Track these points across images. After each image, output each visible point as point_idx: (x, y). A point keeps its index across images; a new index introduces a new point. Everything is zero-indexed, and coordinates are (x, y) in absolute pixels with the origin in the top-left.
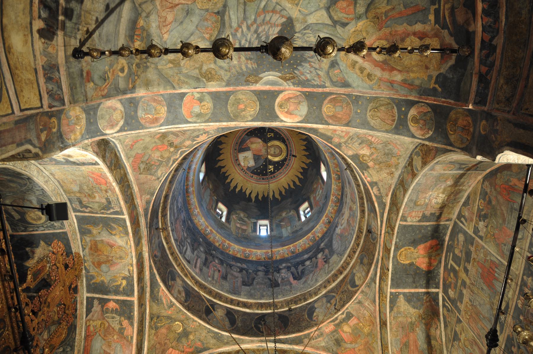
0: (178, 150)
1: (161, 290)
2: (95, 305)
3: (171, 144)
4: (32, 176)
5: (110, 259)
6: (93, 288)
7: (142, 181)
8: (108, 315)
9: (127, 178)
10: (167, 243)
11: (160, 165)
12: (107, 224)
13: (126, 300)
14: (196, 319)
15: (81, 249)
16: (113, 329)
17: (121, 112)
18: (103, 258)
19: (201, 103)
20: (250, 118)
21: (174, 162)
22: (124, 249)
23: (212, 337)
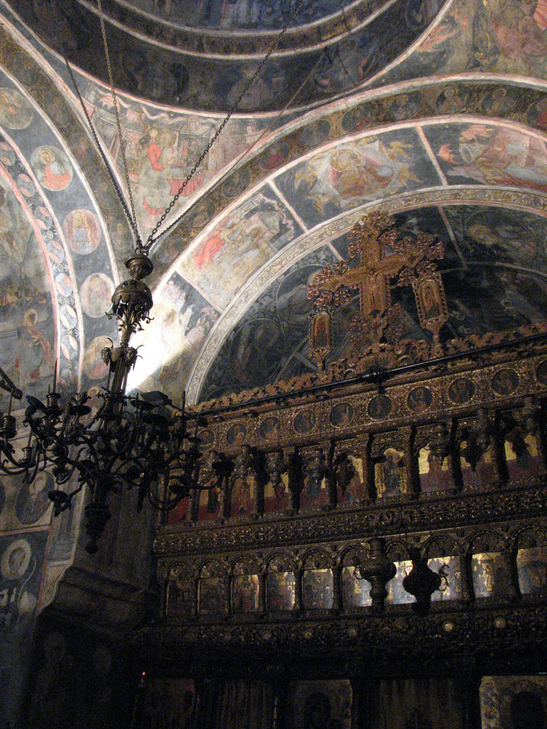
0: (152, 122)
1: (421, 50)
2: (458, 174)
3: (144, 142)
5: (363, 169)
7: (221, 156)
8: (464, 158)
9: (216, 190)
10: (371, 12)
11: (188, 138)
13: (427, 136)
16: (485, 151)
19: (45, 165)
20: (16, 93)
21: (176, 115)
22: (335, 158)
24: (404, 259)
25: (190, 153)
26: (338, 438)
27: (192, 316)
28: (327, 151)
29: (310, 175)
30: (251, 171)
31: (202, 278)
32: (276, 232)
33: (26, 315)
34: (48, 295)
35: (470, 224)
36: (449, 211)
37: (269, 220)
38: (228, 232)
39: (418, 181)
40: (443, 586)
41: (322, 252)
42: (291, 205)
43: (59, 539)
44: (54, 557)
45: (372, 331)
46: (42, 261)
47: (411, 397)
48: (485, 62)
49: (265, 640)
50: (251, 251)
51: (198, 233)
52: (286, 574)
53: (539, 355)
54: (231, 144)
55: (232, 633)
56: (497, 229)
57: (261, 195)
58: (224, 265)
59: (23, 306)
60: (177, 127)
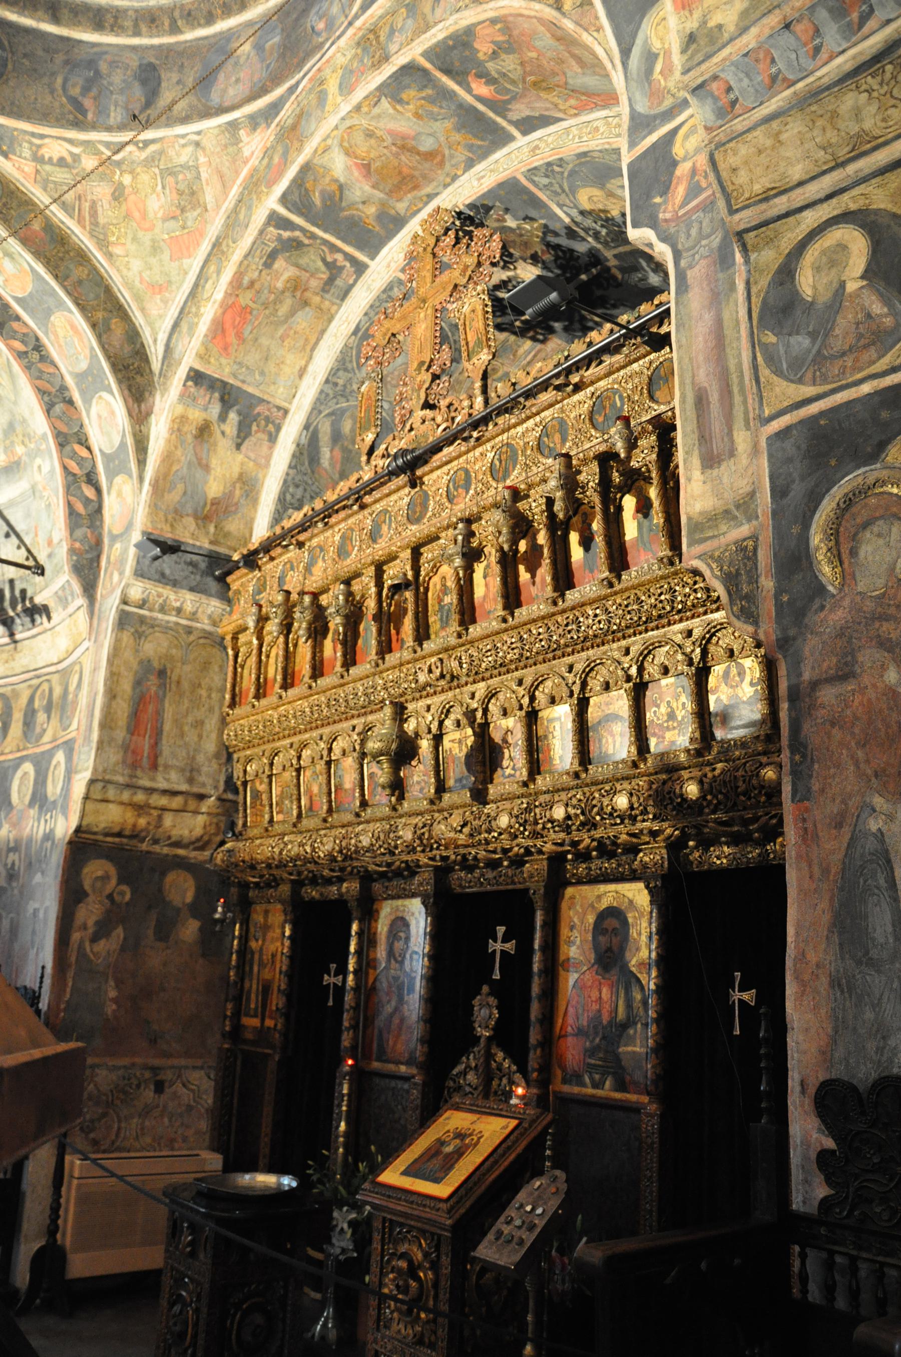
3: (118, 194)
5: (394, 148)
7: (219, 186)
11: (170, 172)
24: (457, 273)
25: (180, 193)
27: (240, 423)
28: (328, 136)
29: (327, 180)
31: (236, 367)
32: (325, 277)
35: (573, 191)
37: (303, 261)
38: (249, 294)
40: (505, 763)
41: (396, 289)
42: (325, 231)
47: (451, 485)
50: (300, 313)
52: (350, 759)
53: (592, 383)
54: (227, 164)
56: (608, 186)
57: (271, 229)
58: (264, 341)
60: (153, 161)
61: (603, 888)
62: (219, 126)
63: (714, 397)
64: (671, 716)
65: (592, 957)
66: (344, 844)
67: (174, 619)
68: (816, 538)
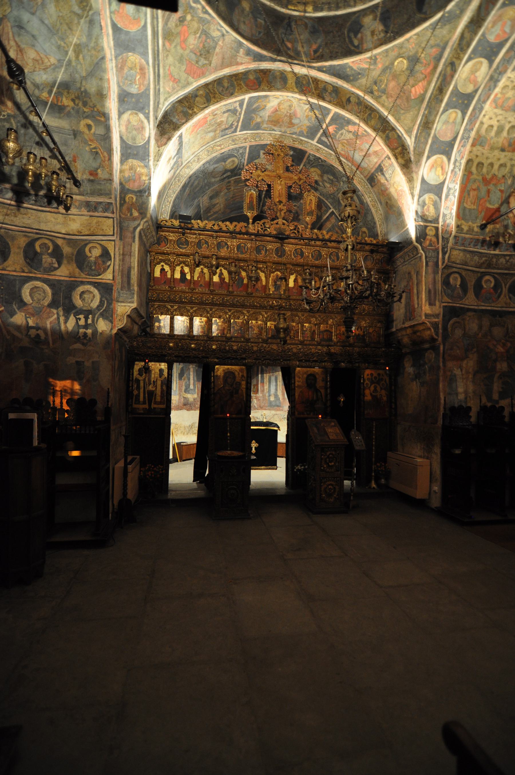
0: (191, 7)
1: (351, 65)
4: (189, 176)
5: (288, 114)
6: (311, 134)
8: (337, 136)
10: (322, 10)
11: (206, 33)
12: (252, 110)
13: (332, 117)
14: (408, 36)
15: (273, 132)
16: (351, 139)
17: (131, 114)
18: (286, 119)
21: (206, 12)
23: (441, 28)
24: (296, 178)
25: (204, 47)
26: (259, 262)
27: (175, 162)
28: (283, 96)
30: (235, 83)
32: (227, 127)
33: (83, 122)
34: (107, 115)
35: (313, 167)
36: (311, 156)
37: (230, 119)
39: (305, 133)
42: (244, 115)
43: (122, 290)
44: (120, 300)
45: (279, 212)
46: (106, 85)
48: (376, 93)
49: (213, 349)
51: (200, 112)
55: (195, 344)
56: (325, 175)
57: (238, 103)
59: (80, 115)
61: (309, 369)
62: (236, 38)
63: (433, 292)
64: (343, 334)
65: (306, 385)
66: (223, 347)
67: (145, 240)
68: (449, 327)
